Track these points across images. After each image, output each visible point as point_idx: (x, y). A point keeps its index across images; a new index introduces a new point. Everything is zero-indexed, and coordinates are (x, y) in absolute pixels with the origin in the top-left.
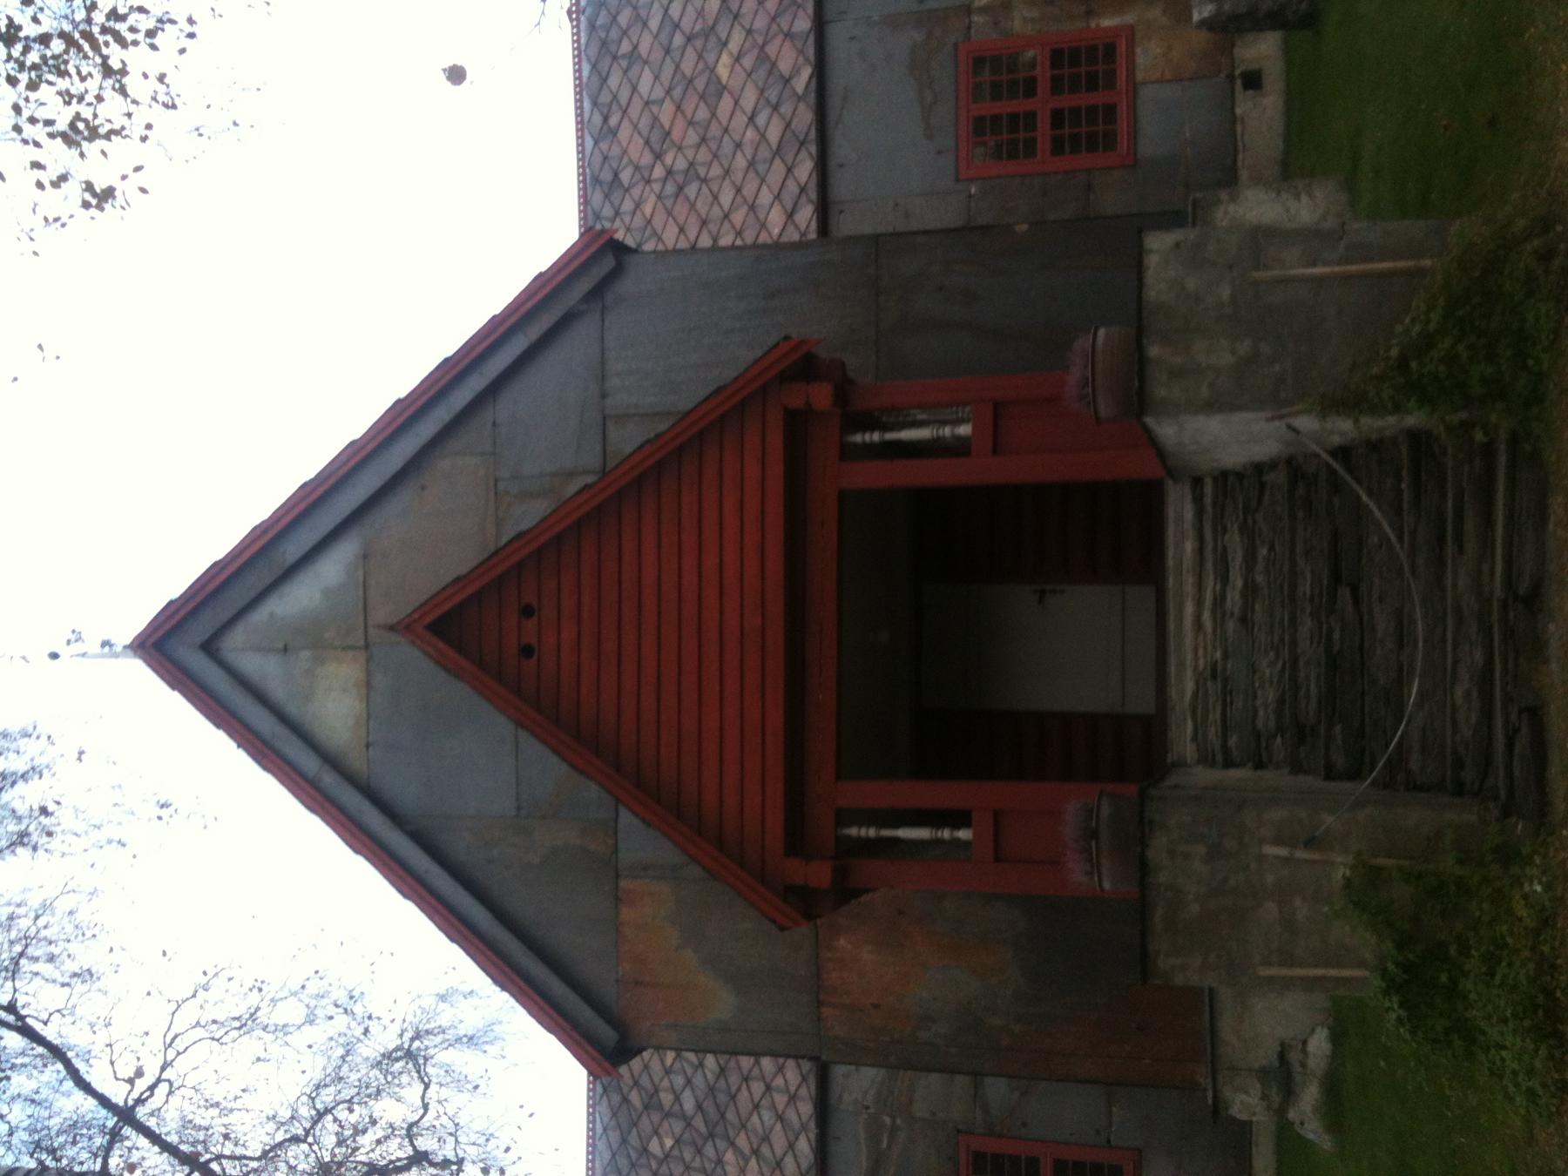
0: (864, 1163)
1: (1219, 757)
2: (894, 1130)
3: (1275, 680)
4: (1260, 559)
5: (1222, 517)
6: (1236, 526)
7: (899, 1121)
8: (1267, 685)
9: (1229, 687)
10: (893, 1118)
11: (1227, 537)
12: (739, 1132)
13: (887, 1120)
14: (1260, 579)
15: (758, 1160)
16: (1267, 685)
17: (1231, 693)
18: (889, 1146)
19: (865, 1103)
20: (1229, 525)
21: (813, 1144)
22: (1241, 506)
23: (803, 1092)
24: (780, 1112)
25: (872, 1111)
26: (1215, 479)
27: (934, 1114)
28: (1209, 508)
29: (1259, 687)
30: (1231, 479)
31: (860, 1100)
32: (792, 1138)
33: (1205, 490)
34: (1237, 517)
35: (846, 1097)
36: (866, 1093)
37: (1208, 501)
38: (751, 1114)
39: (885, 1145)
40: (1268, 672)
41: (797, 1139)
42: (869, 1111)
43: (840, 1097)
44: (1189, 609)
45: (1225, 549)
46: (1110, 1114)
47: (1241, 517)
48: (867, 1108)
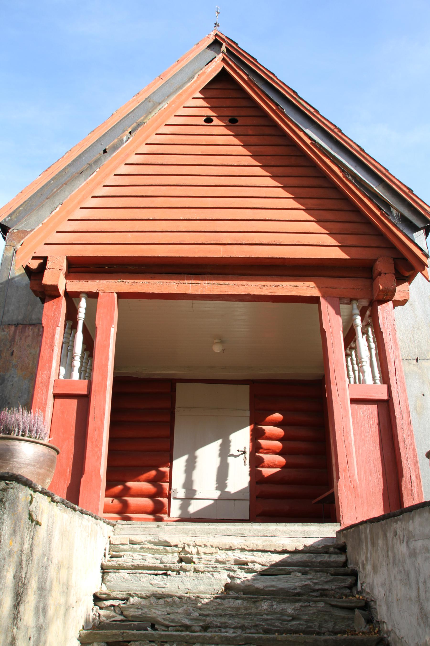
1: (115, 562)
3: (172, 617)
4: (283, 606)
5: (316, 571)
6: (308, 582)
8: (168, 609)
9: (169, 572)
11: (299, 574)
14: (265, 605)
16: (168, 609)
17: (165, 574)
20: (309, 577)
22: (326, 587)
26: (345, 564)
28: (319, 559)
29: (167, 601)
30: (349, 580)
33: (334, 556)
34: (315, 584)
37: (326, 558)
40: (180, 610)
44: (236, 542)
45: (289, 573)
47: (317, 587)
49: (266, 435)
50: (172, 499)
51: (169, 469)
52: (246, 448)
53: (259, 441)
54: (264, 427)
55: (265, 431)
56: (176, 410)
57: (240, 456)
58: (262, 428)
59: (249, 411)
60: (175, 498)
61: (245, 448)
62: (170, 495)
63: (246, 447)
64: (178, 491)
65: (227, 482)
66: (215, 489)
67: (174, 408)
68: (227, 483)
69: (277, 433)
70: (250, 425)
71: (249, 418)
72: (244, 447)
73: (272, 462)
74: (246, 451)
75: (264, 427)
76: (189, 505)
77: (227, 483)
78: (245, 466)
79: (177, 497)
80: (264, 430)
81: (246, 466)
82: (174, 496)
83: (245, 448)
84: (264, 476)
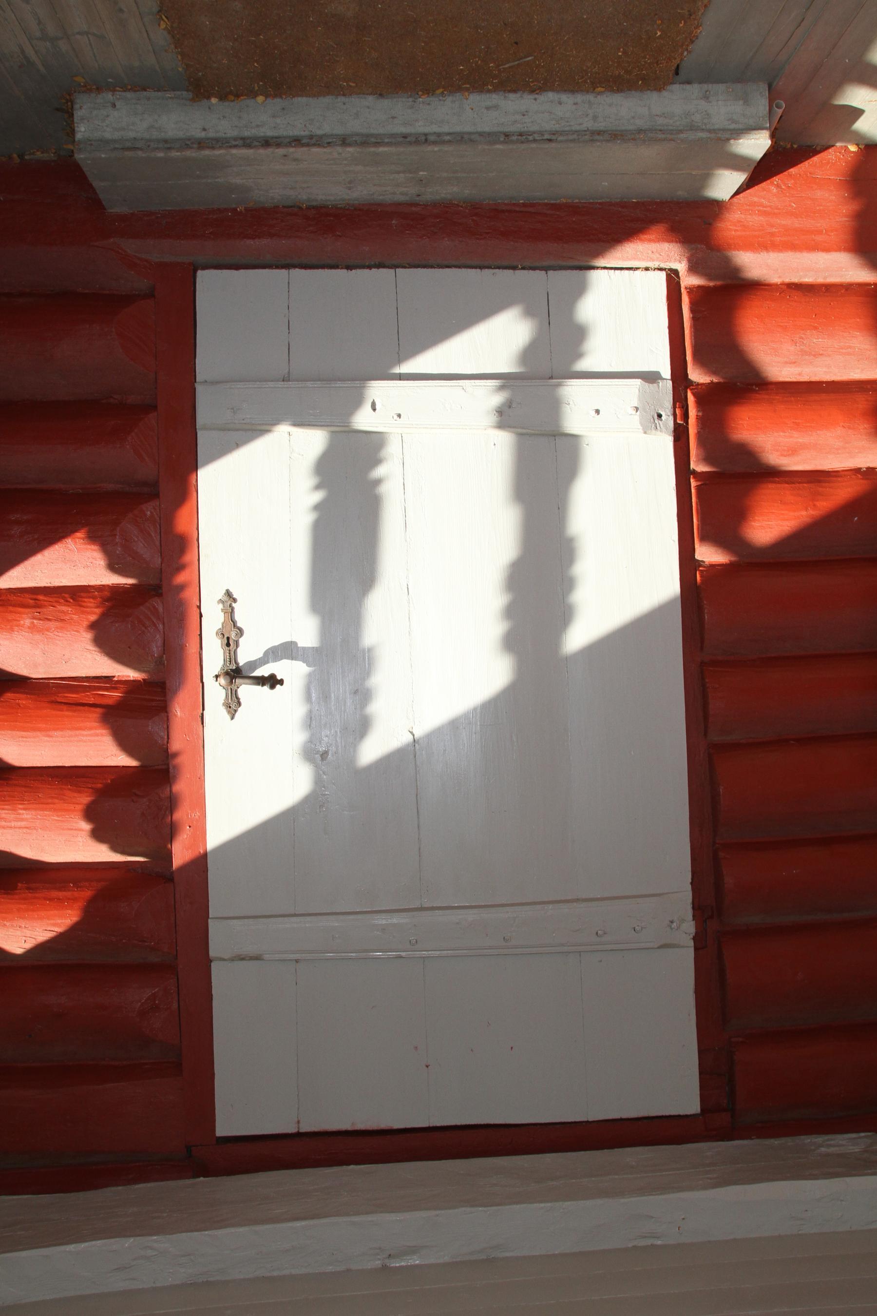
49: (79, 807)
50: (666, 373)
51: (698, 556)
52: (228, 706)
53: (130, 762)
54: (102, 854)
55: (86, 826)
56: (690, 927)
57: (261, 655)
58: (115, 848)
59: (212, 953)
60: (651, 377)
61: (233, 705)
62: (679, 400)
63: (223, 711)
64: (636, 417)
65: (317, 497)
66: (392, 449)
67: (700, 942)
68: (318, 487)
69: (26, 815)
70: (201, 863)
71: (215, 908)
72: (240, 709)
73: (53, 625)
74: (222, 681)
75: (102, 854)
76: (528, 354)
77: (318, 487)
78: (228, 594)
79: (638, 382)
80: (98, 835)
81: (221, 594)
82: (653, 387)
83: (233, 705)
84: (92, 538)
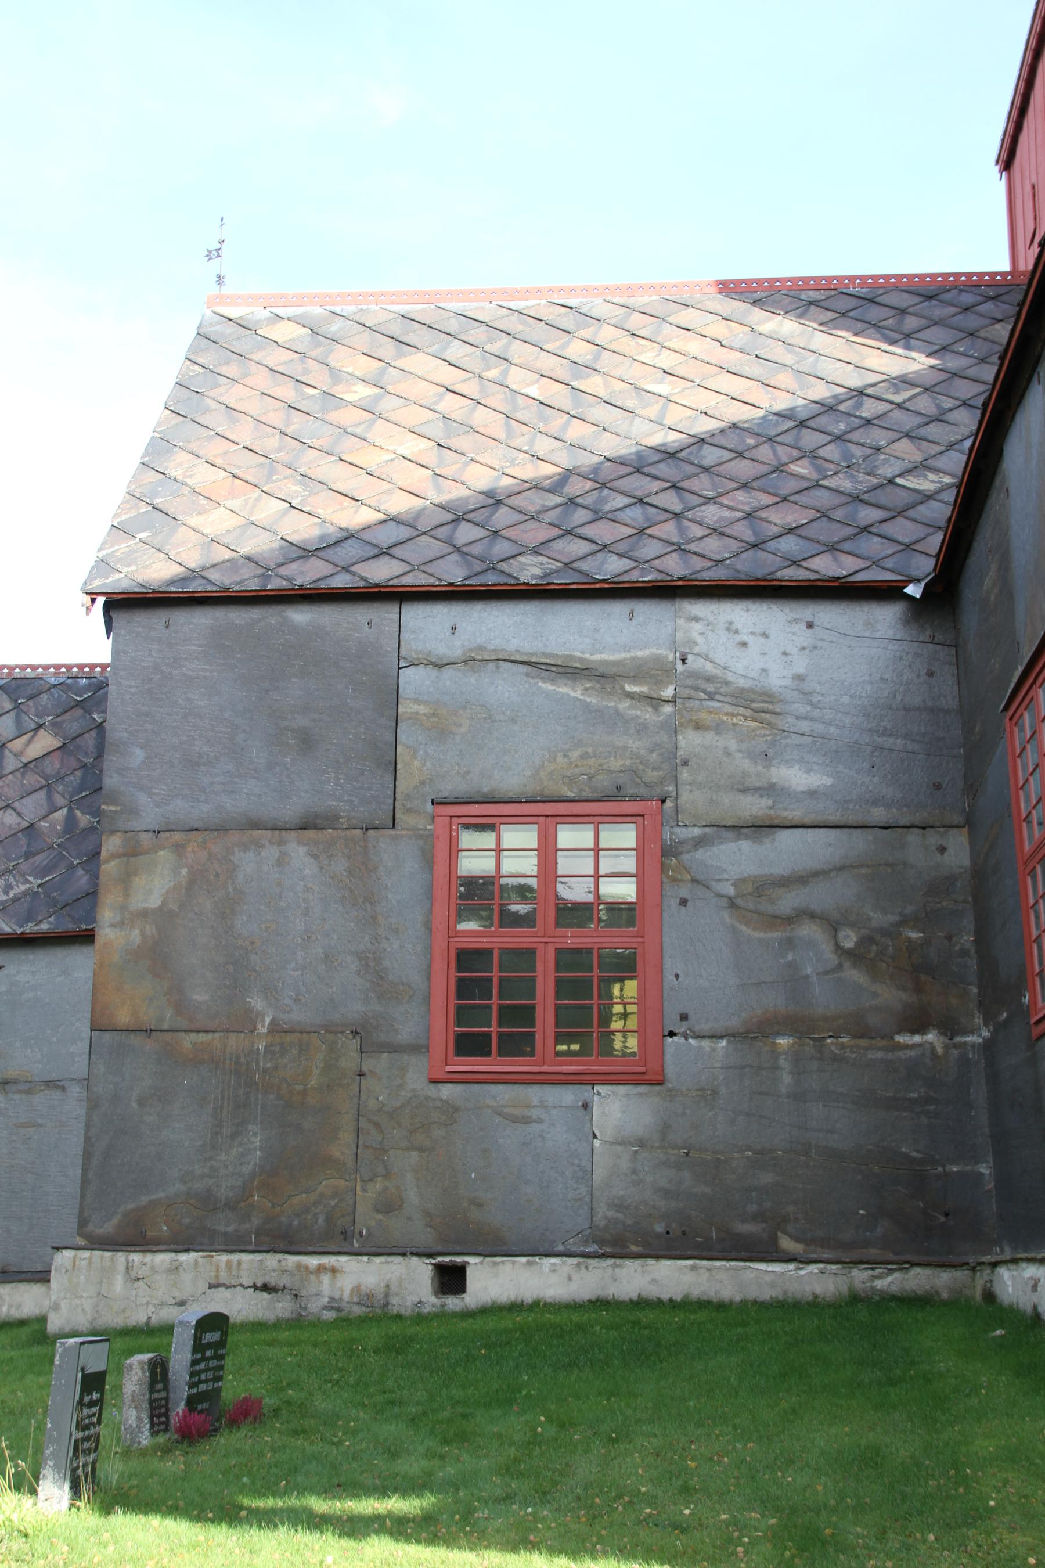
0: (597, 657)
2: (655, 702)
7: (668, 709)
10: (673, 701)
12: (590, 479)
13: (669, 692)
15: (561, 505)
18: (630, 696)
19: (689, 657)
21: (625, 578)
23: (698, 563)
24: (648, 531)
25: (680, 666)
27: (685, 763)
31: (696, 650)
32: (622, 547)
35: (697, 627)
36: (707, 658)
38: (624, 494)
39: (628, 688)
41: (621, 555)
42: (679, 663)
43: (696, 619)
46: (714, 1036)
48: (684, 661)
